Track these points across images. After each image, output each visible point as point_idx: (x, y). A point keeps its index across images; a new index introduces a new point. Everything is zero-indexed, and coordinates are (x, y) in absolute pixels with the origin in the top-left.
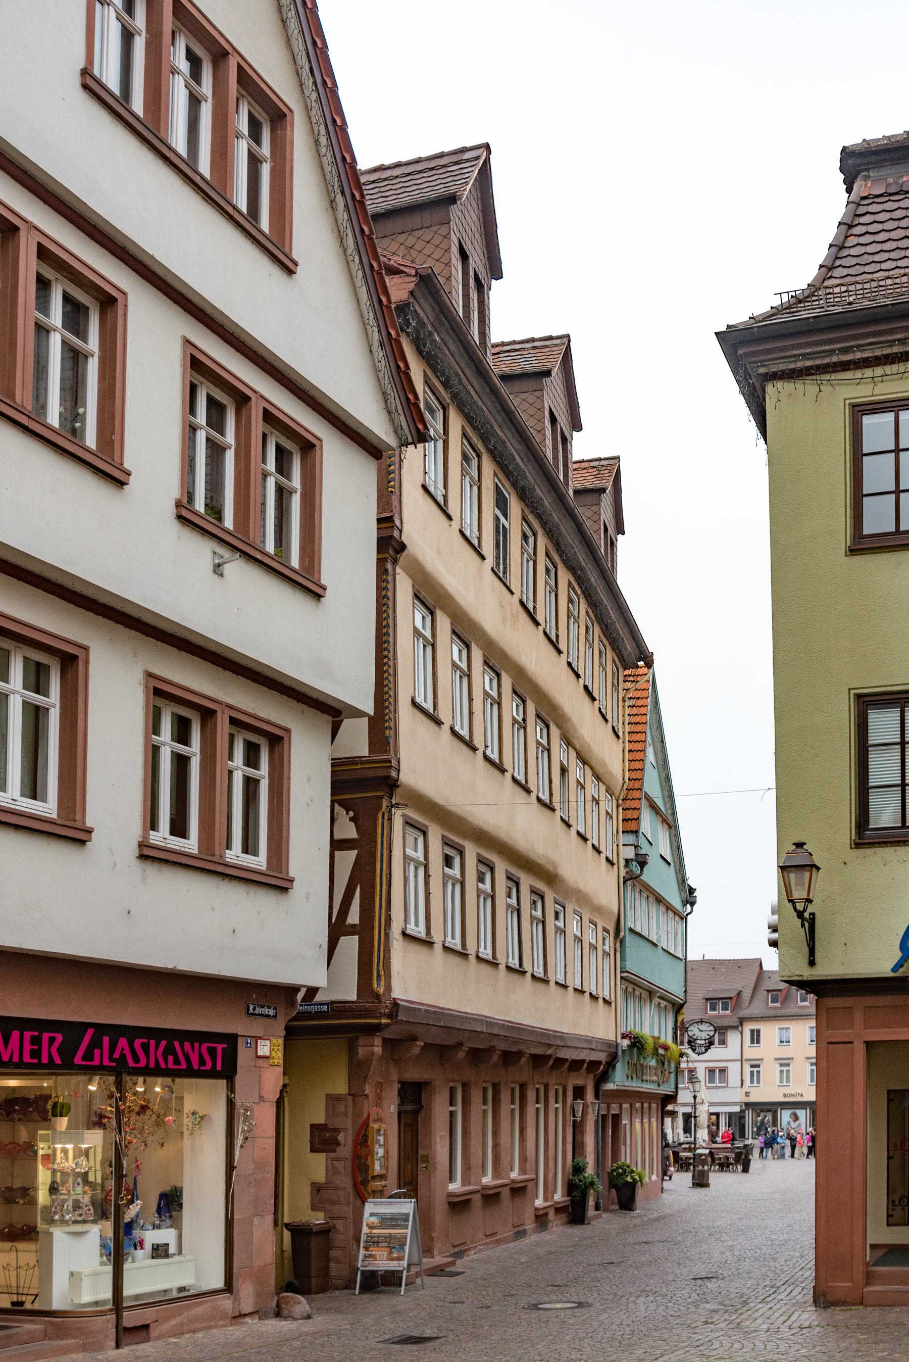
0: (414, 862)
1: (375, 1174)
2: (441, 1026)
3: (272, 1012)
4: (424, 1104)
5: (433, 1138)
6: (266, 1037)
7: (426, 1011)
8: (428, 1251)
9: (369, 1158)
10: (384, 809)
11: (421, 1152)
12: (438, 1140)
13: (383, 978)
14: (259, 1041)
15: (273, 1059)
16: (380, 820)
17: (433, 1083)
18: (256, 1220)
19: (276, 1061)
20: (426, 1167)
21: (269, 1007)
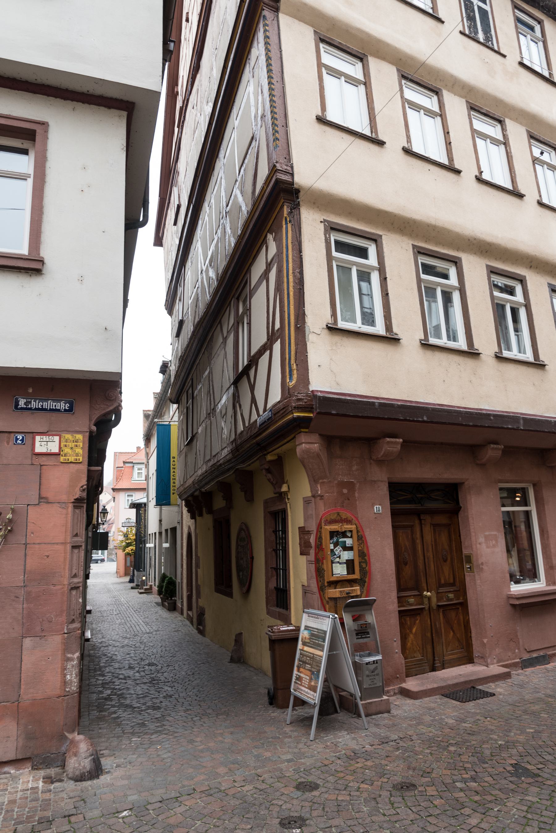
0: (357, 266)
1: (332, 579)
2: (424, 422)
3: (62, 406)
4: (461, 505)
5: (473, 539)
6: (54, 433)
7: (380, 404)
8: (482, 657)
9: (324, 561)
10: (285, 215)
11: (465, 552)
12: (482, 539)
13: (295, 372)
14: (38, 438)
15: (65, 455)
16: (284, 226)
17: (466, 483)
18: (28, 642)
19: (72, 459)
20: (470, 568)
21: (59, 401)
